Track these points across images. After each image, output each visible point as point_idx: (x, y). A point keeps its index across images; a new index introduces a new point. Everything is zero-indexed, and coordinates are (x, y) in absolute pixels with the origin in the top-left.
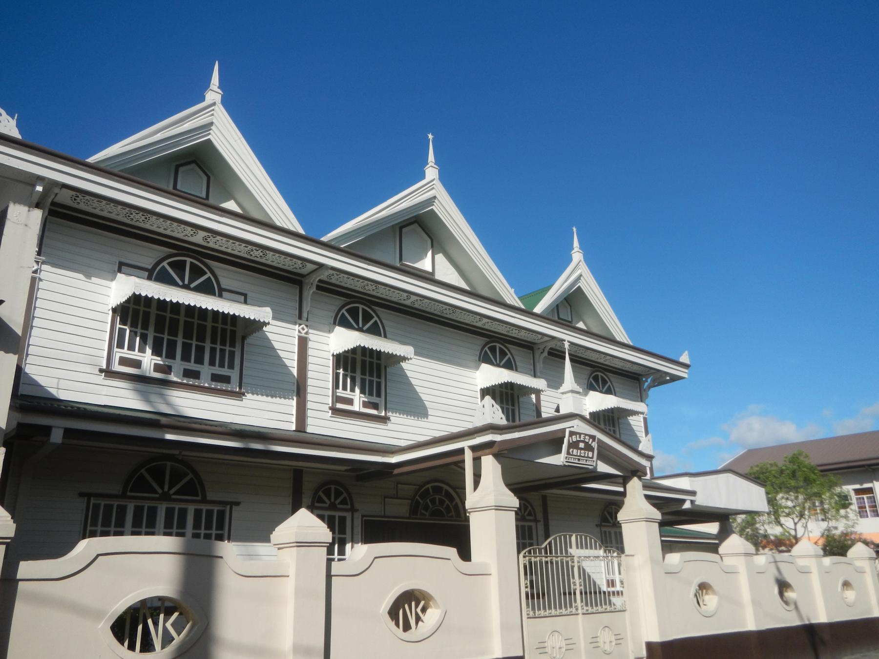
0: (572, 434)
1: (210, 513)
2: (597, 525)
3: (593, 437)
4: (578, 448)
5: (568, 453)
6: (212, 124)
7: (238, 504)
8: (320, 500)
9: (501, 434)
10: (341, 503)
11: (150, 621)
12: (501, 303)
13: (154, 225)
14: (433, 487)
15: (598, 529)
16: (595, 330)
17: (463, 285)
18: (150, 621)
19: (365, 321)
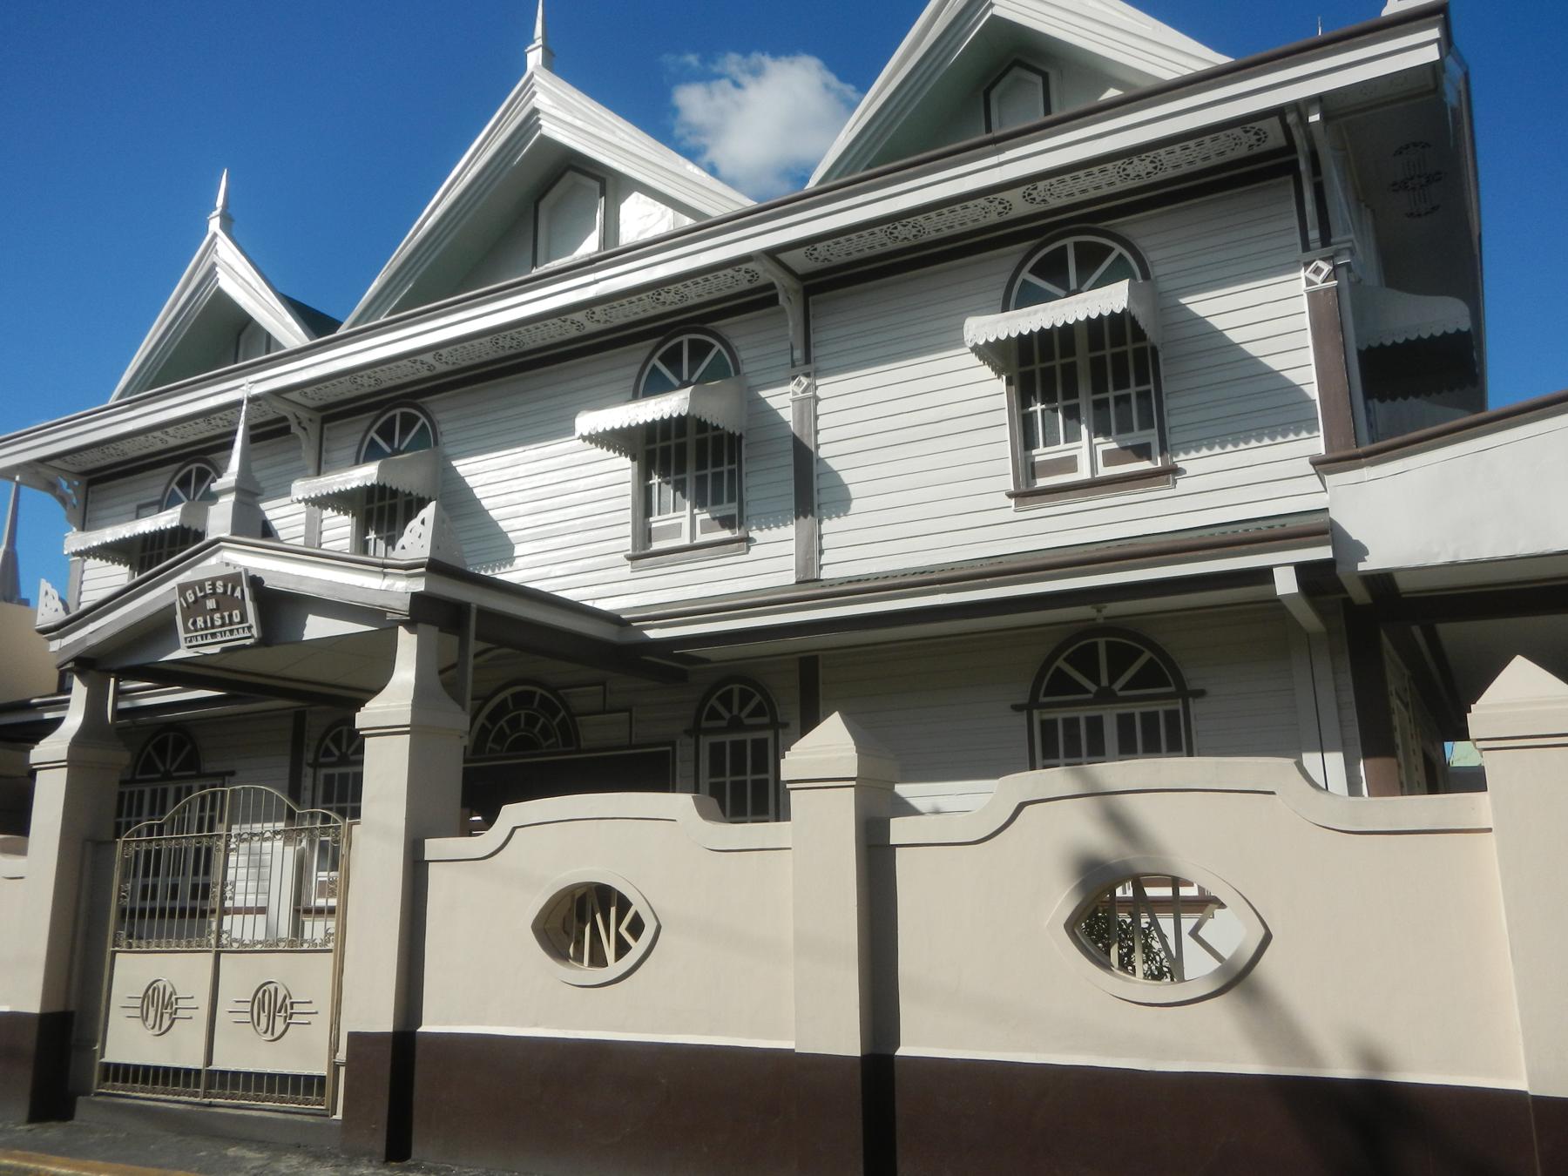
0: (183, 588)
1: (738, 747)
2: (1017, 708)
3: (233, 579)
4: (205, 612)
5: (187, 630)
6: (214, 265)
7: (232, 773)
8: (328, 753)
9: (62, 636)
10: (752, 715)
11: (598, 916)
12: (705, 227)
13: (156, 443)
14: (514, 696)
15: (1022, 719)
16: (1147, 85)
17: (688, 222)
18: (598, 916)
19: (405, 431)
